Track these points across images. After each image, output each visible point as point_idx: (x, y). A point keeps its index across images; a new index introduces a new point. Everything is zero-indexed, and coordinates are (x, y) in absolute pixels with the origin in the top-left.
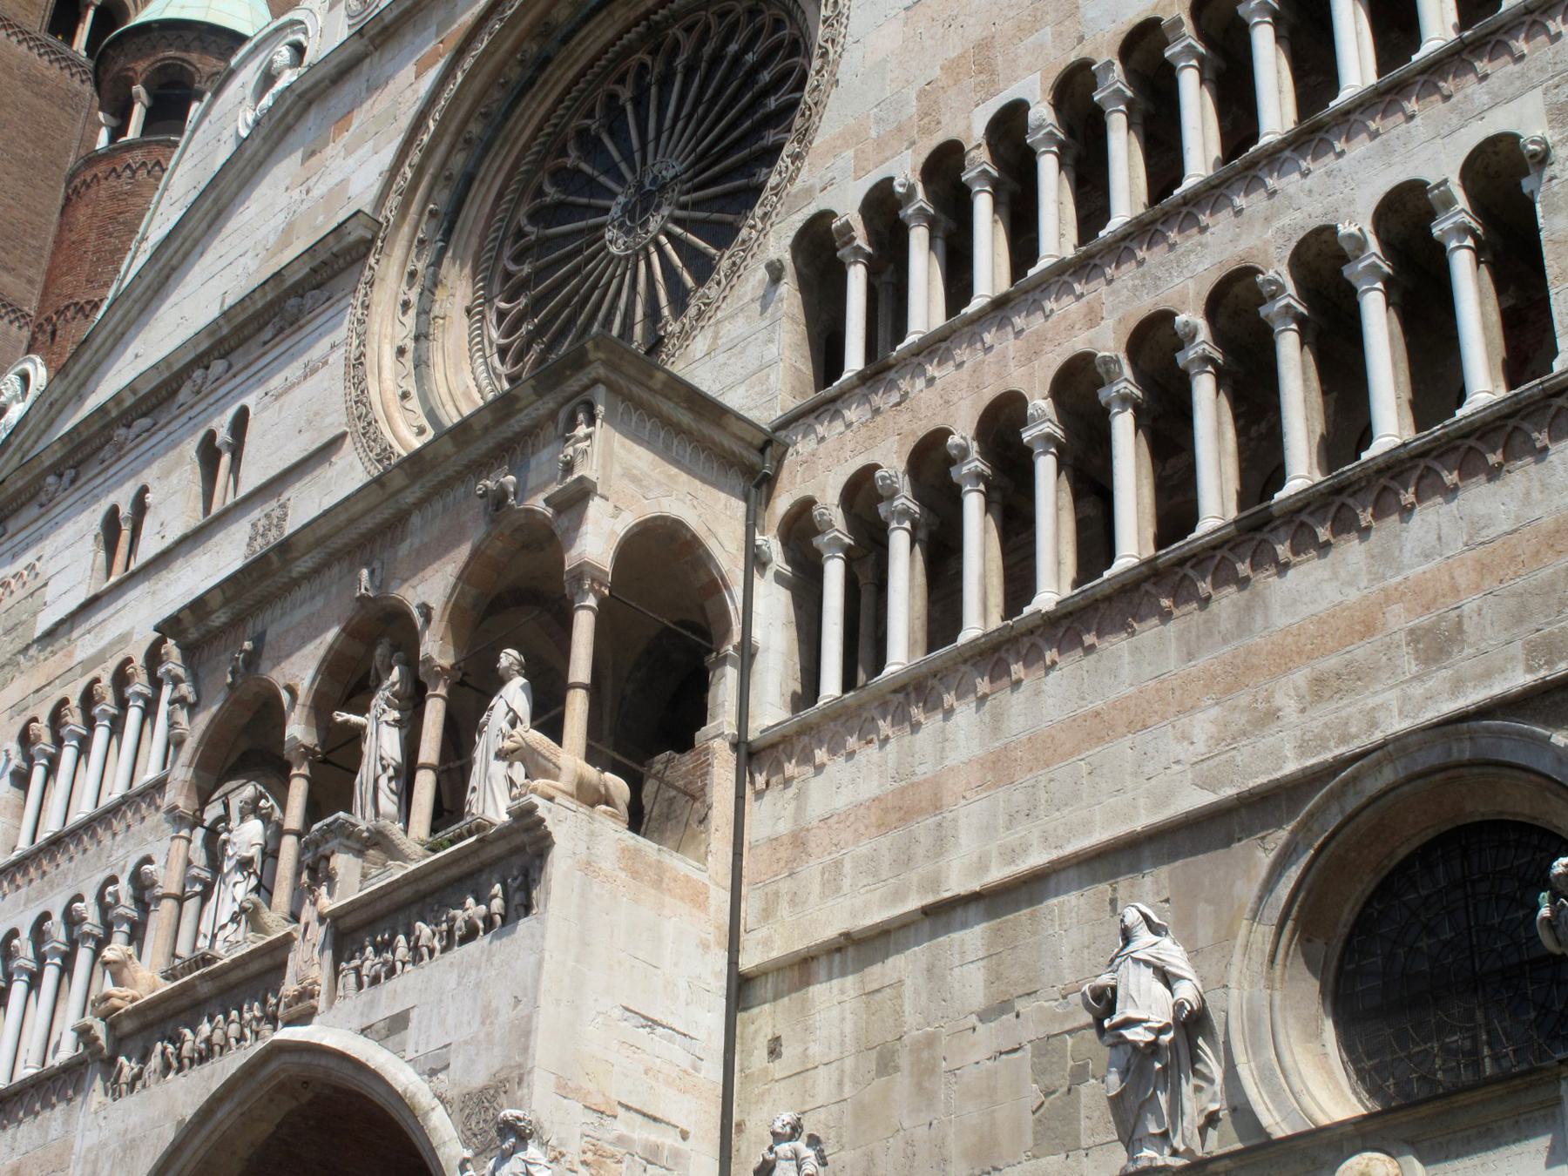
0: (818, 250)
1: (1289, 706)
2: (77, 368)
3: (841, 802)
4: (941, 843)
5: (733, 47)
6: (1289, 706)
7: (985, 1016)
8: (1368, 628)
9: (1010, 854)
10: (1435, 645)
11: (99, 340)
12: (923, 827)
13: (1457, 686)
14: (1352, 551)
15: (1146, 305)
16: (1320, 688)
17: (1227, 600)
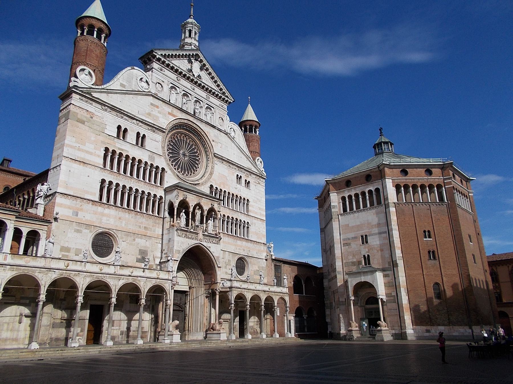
5: (194, 147)
10: (244, 250)
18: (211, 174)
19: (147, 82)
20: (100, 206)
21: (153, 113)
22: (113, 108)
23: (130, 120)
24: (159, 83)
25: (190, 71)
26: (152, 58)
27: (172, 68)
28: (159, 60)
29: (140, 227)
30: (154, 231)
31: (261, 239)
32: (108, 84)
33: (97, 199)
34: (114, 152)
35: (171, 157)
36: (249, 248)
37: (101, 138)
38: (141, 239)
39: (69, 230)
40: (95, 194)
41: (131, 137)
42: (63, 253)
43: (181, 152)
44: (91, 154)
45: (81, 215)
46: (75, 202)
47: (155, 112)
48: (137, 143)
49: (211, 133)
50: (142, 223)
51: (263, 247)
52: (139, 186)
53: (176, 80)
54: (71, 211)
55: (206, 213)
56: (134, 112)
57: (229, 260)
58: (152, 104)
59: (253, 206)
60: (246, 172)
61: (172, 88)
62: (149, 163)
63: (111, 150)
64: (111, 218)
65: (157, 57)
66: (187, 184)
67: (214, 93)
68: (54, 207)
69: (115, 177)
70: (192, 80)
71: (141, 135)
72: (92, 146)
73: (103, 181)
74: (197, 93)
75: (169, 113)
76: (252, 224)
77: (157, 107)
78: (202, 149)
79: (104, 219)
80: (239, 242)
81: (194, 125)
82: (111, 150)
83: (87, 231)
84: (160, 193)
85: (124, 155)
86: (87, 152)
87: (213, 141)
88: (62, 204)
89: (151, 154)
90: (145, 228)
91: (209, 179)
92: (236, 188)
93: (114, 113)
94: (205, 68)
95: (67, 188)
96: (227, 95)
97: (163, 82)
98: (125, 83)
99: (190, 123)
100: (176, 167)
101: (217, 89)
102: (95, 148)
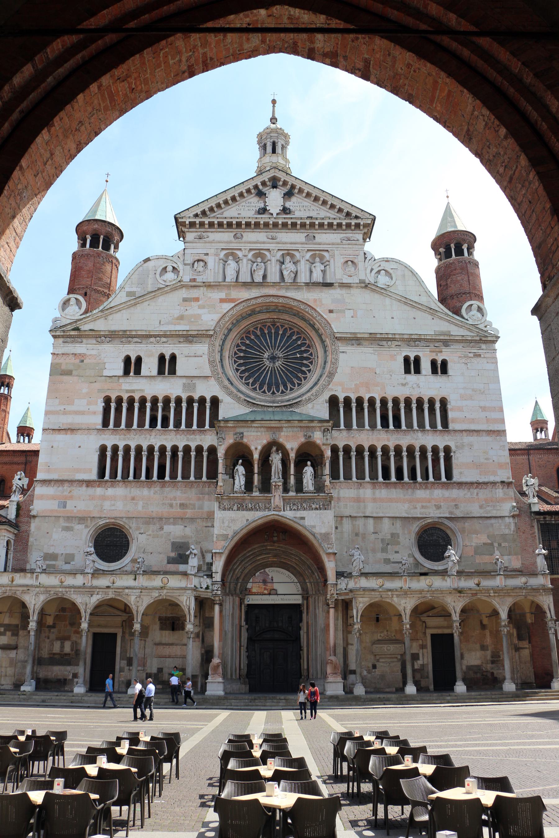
0: (333, 401)
1: (419, 508)
2: (107, 312)
3: (347, 496)
4: (365, 507)
5: (294, 338)
6: (419, 508)
7: (373, 533)
8: (429, 502)
9: (377, 513)
10: (438, 507)
11: (115, 309)
12: (362, 504)
13: (440, 513)
14: (428, 492)
15: (397, 443)
16: (423, 507)
17: (410, 491)
18: (331, 375)
19: (174, 268)
20: (99, 486)
21: (190, 312)
22: (113, 336)
23: (144, 342)
24: (198, 261)
25: (263, 211)
26: (183, 229)
27: (220, 225)
28: (192, 225)
29: (171, 506)
30: (201, 507)
31: (495, 474)
32: (105, 304)
33: (93, 475)
34: (119, 400)
35: (243, 372)
36: (454, 500)
37: (97, 386)
38: (174, 524)
39: (55, 530)
40: (90, 470)
41: (150, 366)
42: (48, 562)
43: (266, 355)
44: (82, 413)
45: (70, 505)
46: (60, 488)
47: (193, 309)
48: (161, 372)
49: (320, 301)
50: (175, 498)
51: (500, 492)
52: (166, 439)
53: (232, 239)
54: (56, 502)
55: (292, 455)
56: (153, 326)
57: (393, 535)
58: (185, 300)
59: (460, 409)
60: (432, 345)
61: (227, 255)
62: (184, 397)
63: (113, 398)
64: (119, 502)
65: (187, 223)
66: (270, 409)
67: (321, 225)
68: (33, 501)
69: (122, 436)
70: (266, 225)
71: (167, 358)
72: (84, 402)
73: (103, 449)
74: (284, 240)
75: (222, 301)
76: (461, 447)
77: (197, 299)
78: (313, 334)
79: (107, 505)
80: (421, 494)
81: (281, 300)
82: (113, 398)
83: (81, 527)
84: (207, 439)
85: (137, 398)
86: (77, 413)
87: (331, 311)
88: (42, 495)
89: (189, 381)
90: (182, 505)
91: (325, 387)
92: (404, 385)
93: (117, 341)
94: (296, 191)
95: (49, 471)
96: (354, 215)
97: (207, 254)
98: (134, 289)
99: (271, 299)
100: (257, 385)
101: (332, 214)
102: (89, 403)
